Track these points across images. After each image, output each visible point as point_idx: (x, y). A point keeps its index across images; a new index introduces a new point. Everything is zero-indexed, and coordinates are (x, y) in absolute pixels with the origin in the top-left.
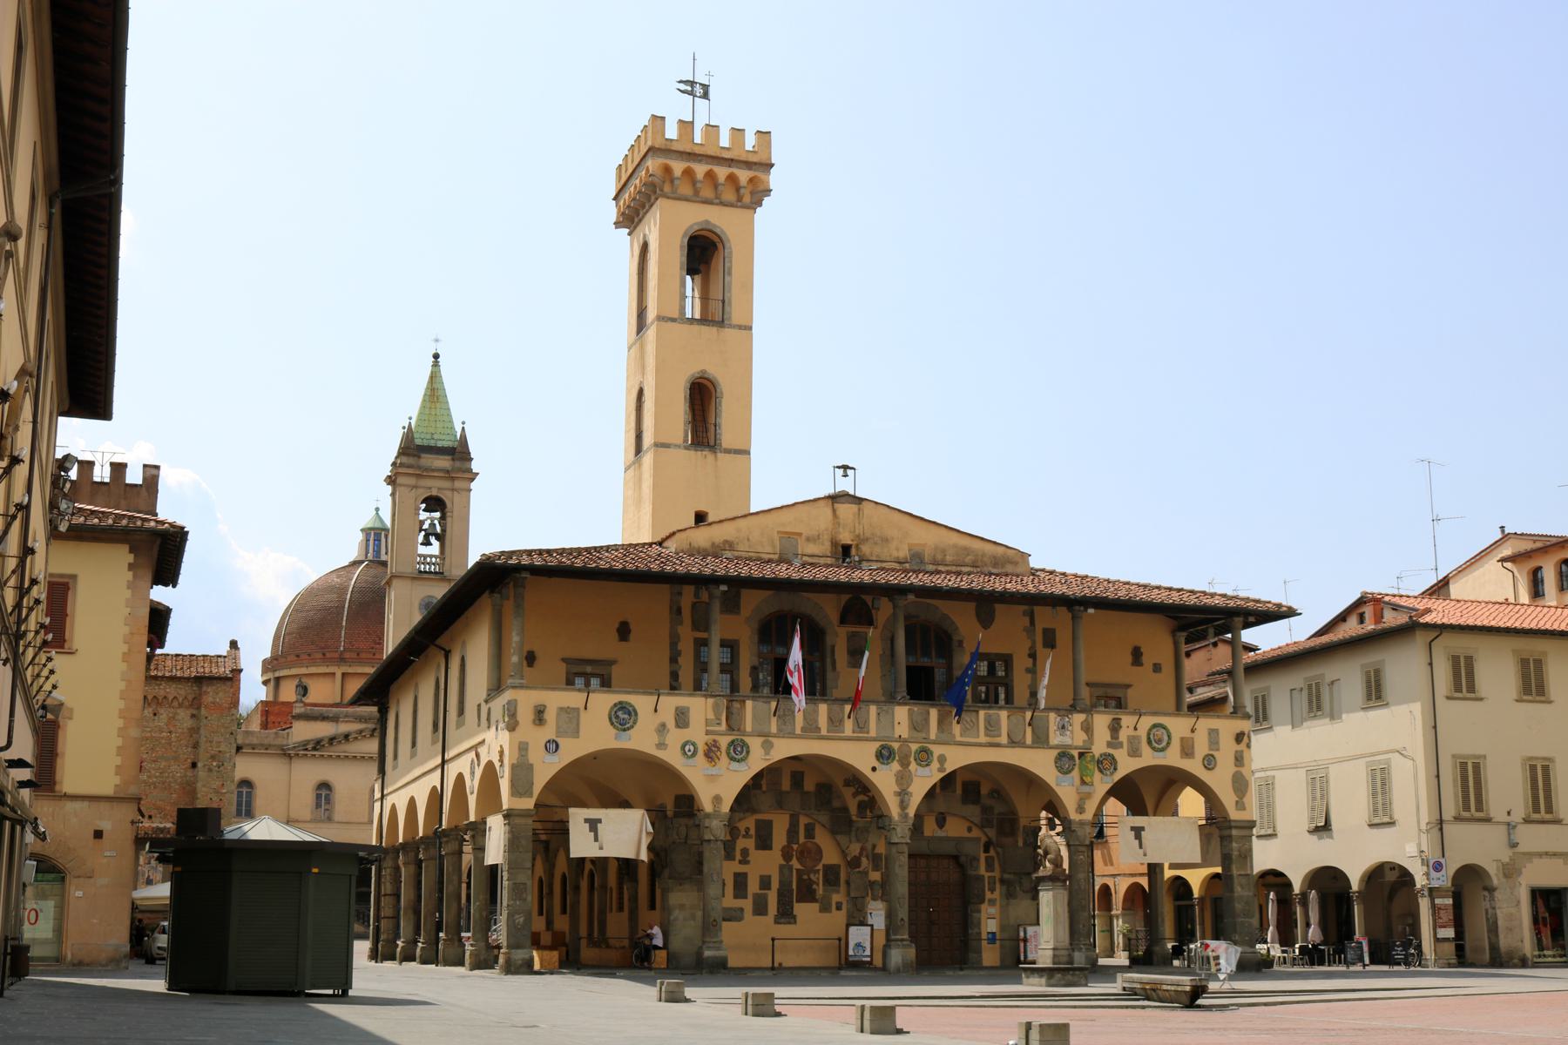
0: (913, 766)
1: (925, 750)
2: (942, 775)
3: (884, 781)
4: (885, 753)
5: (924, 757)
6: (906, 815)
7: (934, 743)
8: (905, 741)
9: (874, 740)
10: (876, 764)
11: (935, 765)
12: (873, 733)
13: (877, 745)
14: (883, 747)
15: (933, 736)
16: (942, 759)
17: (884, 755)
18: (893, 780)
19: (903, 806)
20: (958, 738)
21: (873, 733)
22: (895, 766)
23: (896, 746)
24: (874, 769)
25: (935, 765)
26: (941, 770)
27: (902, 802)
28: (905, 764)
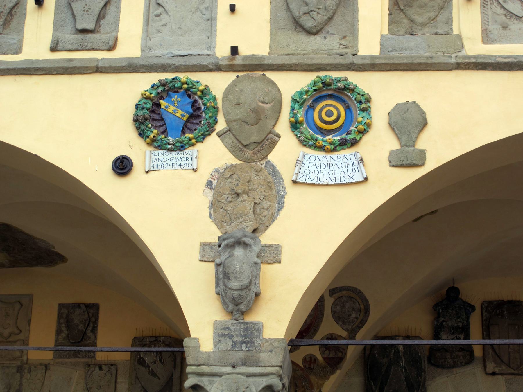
0: (286, 152)
1: (342, 93)
2: (409, 177)
3: (168, 210)
4: (174, 109)
5: (334, 115)
6: (251, 335)
7: (372, 66)
8: (256, 66)
9: (131, 67)
10: (137, 150)
11: (380, 142)
12: (130, 42)
13: (145, 82)
14: (166, 89)
15: (369, 45)
16: (409, 122)
17: (171, 116)
18: (202, 200)
19: (238, 299)
20: (475, 47)
21: (130, 47)
22: (213, 153)
23: (218, 84)
24: (122, 166)
25: (380, 142)
26: (405, 158)
27: (223, 275)
28: (253, 143)
